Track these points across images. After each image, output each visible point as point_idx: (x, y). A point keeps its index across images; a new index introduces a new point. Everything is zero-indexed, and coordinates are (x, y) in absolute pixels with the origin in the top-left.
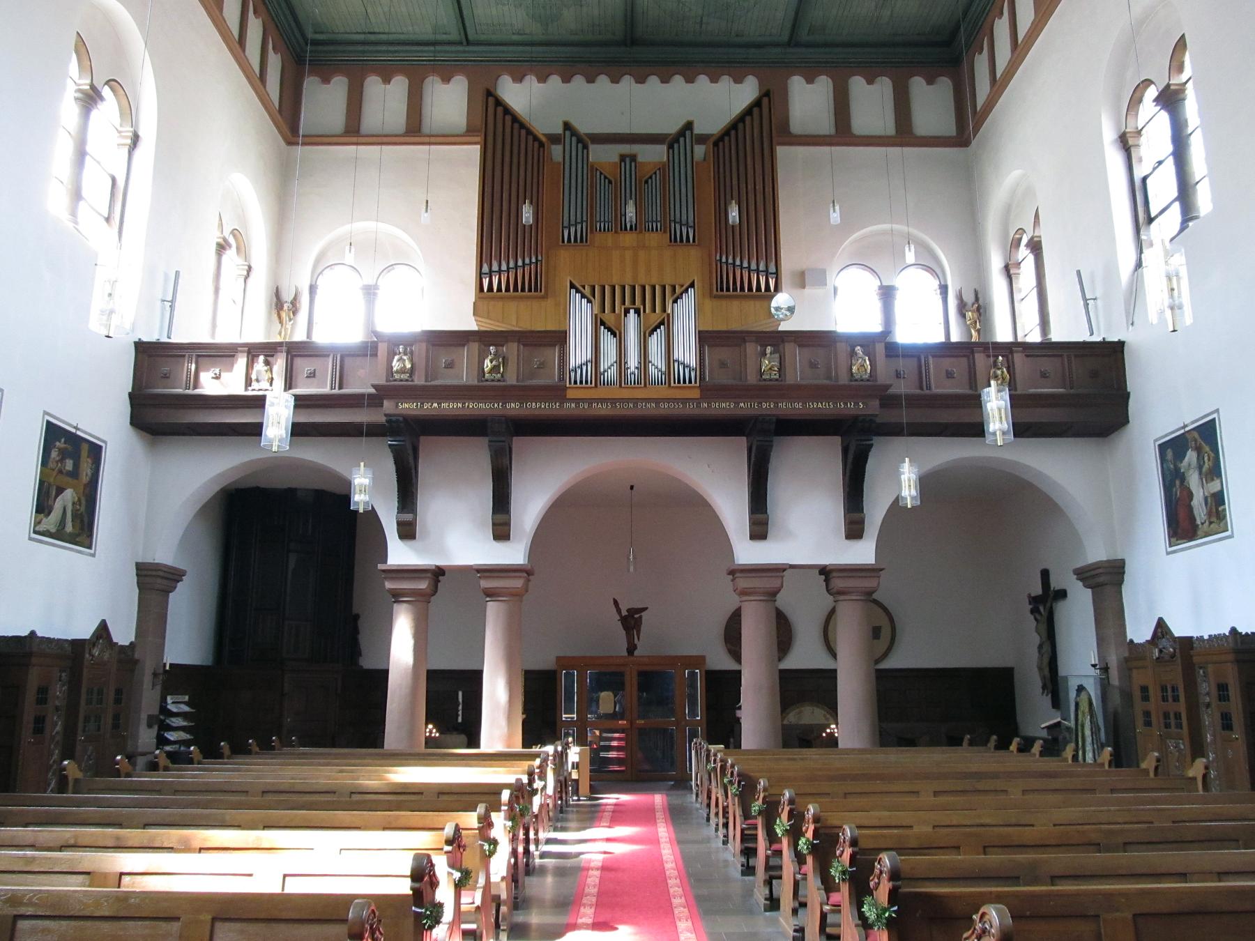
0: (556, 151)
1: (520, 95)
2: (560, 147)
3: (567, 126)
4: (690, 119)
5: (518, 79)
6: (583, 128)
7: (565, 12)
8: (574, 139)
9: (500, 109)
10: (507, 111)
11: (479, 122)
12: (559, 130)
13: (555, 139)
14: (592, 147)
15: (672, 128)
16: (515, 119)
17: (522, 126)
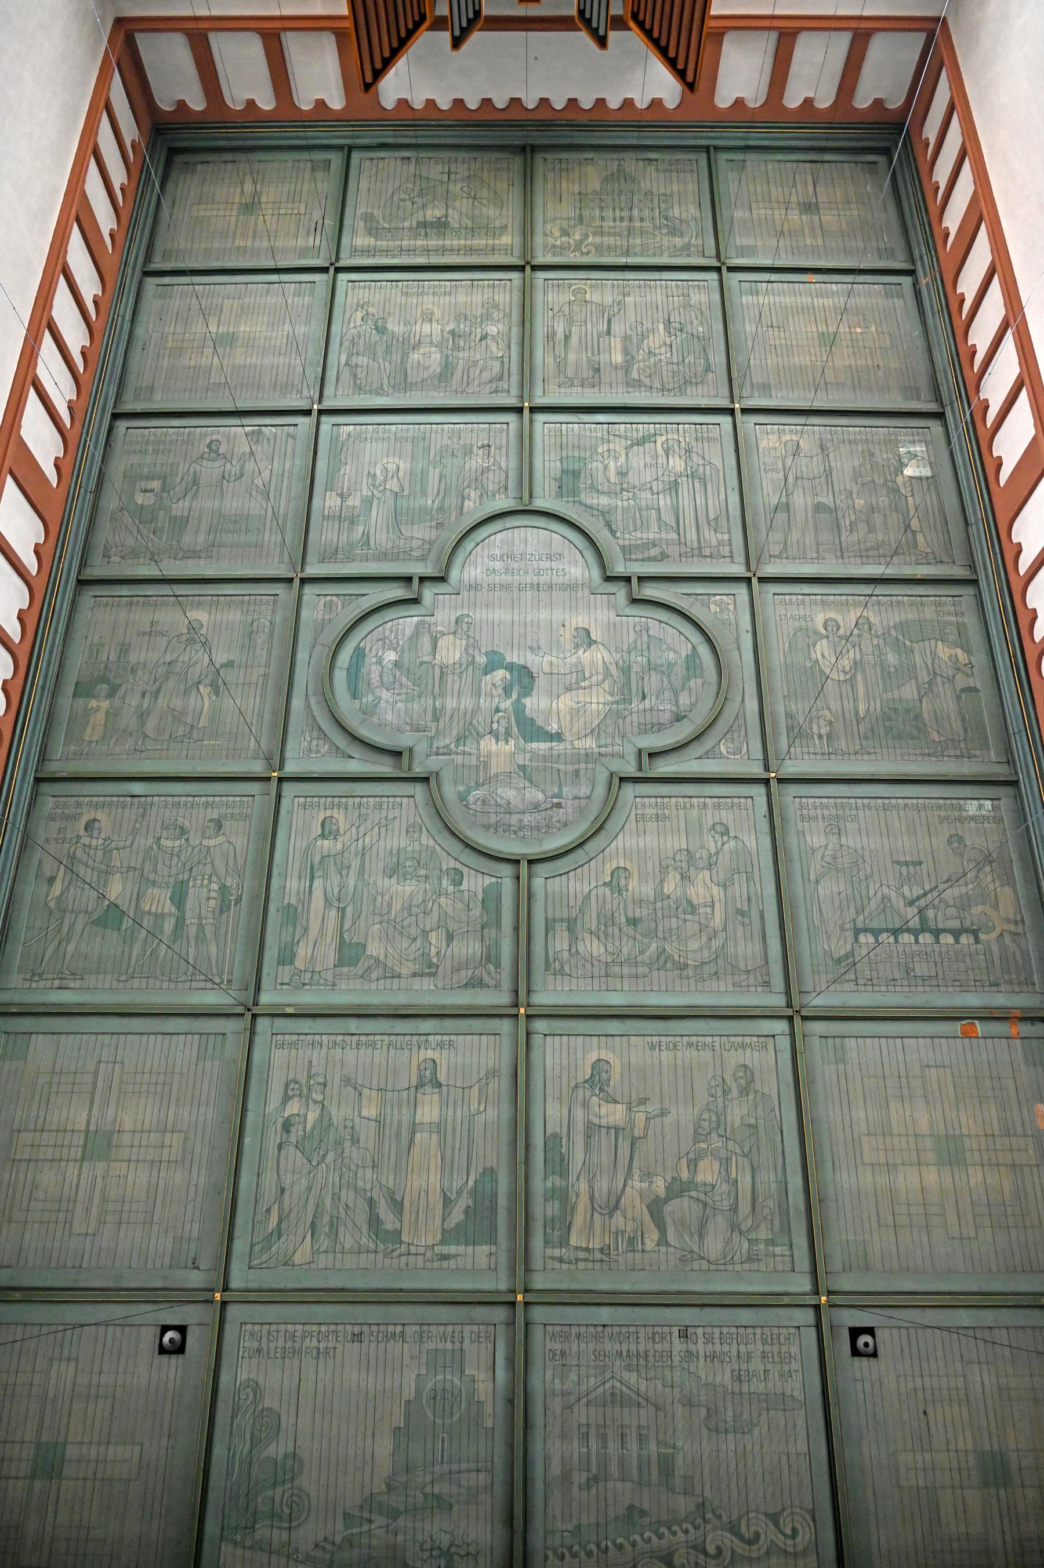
0: (617, 9)
1: (655, 83)
2: (613, 12)
3: (602, 42)
4: (455, 53)
5: (656, 103)
6: (583, 38)
7: (597, 186)
8: (594, 25)
9: (680, 66)
10: (672, 63)
11: (708, 48)
12: (613, 36)
13: (618, 23)
14: (574, 12)
15: (477, 37)
16: (663, 52)
17: (656, 42)
